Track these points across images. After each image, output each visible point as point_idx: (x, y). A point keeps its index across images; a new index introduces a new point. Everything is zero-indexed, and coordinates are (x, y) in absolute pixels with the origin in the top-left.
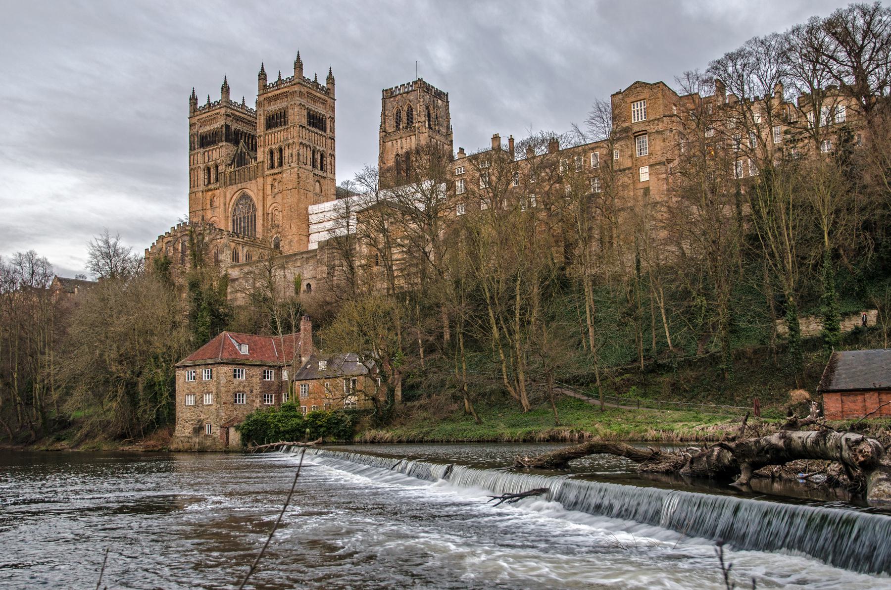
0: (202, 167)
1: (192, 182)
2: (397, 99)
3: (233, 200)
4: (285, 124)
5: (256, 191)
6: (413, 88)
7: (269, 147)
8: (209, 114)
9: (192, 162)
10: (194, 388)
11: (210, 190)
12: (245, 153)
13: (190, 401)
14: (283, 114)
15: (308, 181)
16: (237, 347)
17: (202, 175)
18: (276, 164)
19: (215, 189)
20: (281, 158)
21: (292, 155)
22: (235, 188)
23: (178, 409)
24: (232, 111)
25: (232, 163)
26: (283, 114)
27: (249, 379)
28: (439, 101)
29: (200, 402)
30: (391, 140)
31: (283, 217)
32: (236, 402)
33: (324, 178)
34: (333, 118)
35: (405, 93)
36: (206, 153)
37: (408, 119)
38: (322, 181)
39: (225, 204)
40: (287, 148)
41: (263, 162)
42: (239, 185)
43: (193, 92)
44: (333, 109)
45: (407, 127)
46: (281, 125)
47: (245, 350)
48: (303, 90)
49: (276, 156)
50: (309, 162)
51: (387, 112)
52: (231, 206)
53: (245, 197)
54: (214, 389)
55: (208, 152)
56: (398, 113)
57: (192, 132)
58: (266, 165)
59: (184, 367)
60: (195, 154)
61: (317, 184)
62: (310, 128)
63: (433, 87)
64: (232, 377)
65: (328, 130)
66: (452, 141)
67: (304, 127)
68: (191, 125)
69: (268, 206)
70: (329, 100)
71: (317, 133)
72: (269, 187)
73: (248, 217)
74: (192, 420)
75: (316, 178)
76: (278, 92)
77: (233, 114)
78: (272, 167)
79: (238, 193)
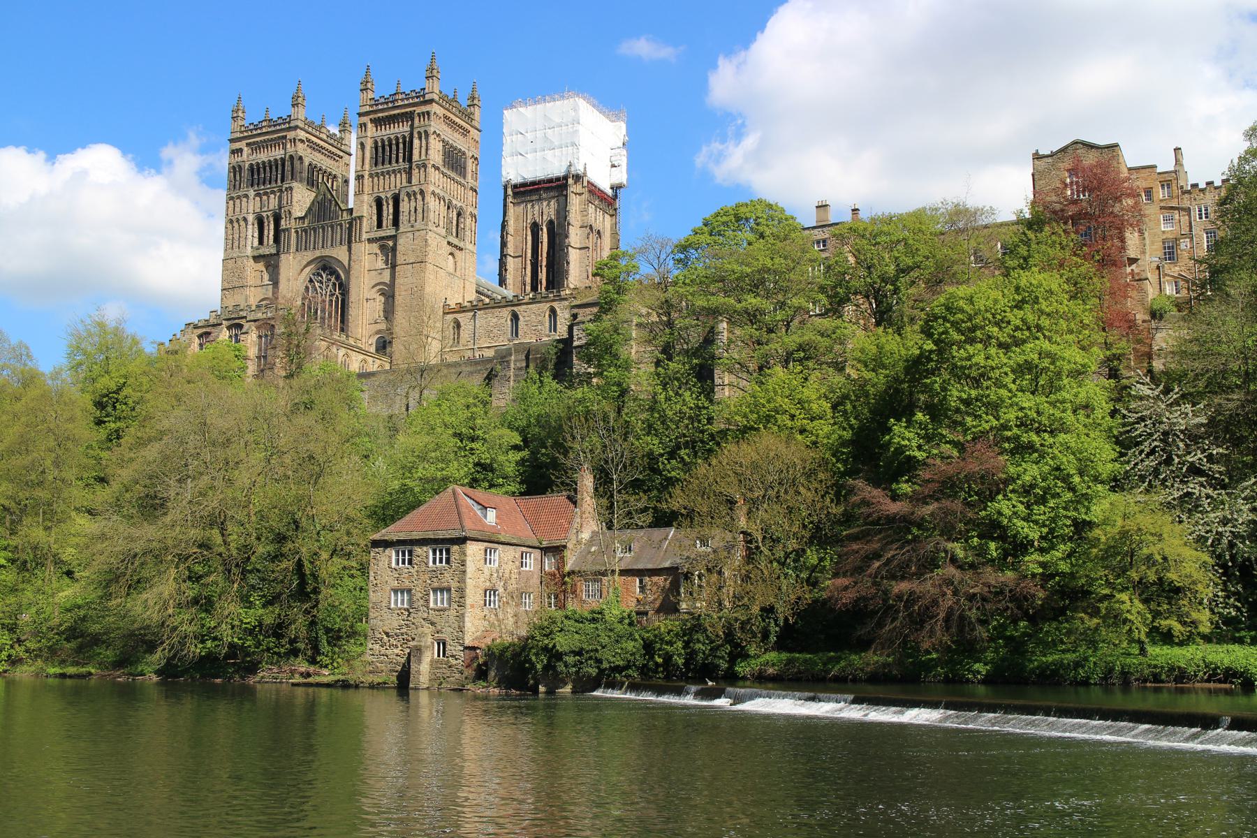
7: (375, 195)
9: (231, 209)
15: (440, 252)
22: (309, 255)
24: (308, 135)
33: (461, 249)
38: (457, 253)
39: (289, 280)
40: (406, 199)
41: (360, 218)
47: (491, 516)
48: (438, 112)
49: (388, 211)
50: (441, 223)
60: (239, 197)
61: (450, 257)
64: (483, 561)
65: (469, 176)
67: (438, 169)
75: (450, 249)
77: (309, 141)
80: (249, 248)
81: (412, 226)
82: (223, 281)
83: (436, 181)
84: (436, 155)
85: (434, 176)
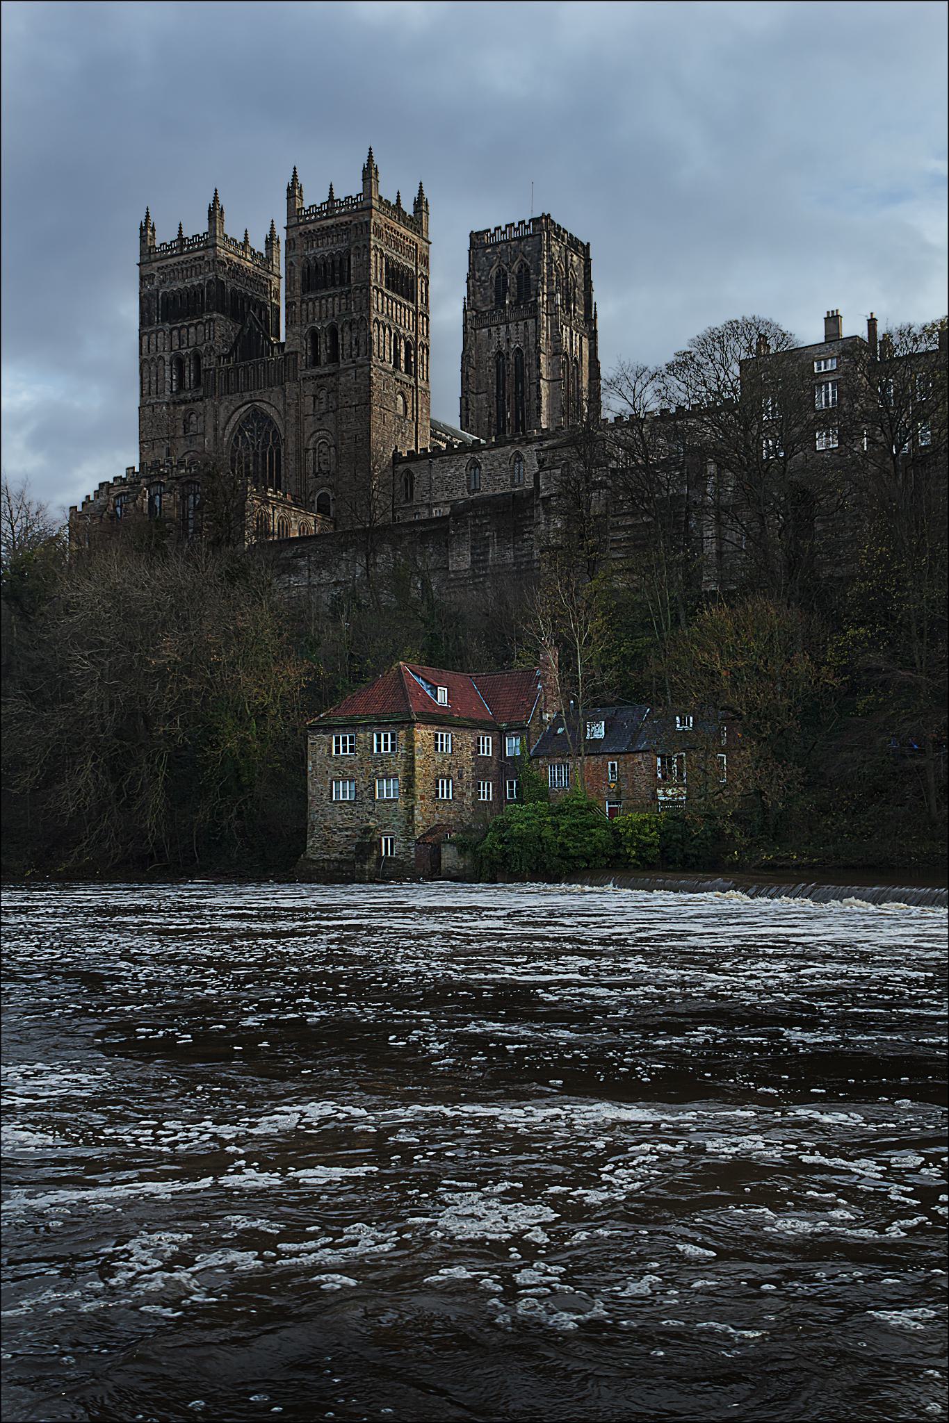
0: (167, 358)
1: (146, 386)
2: (498, 250)
3: (232, 422)
4: (342, 284)
5: (281, 407)
6: (530, 231)
7: (309, 326)
8: (182, 258)
10: (351, 768)
11: (184, 402)
12: (258, 334)
13: (343, 792)
14: (337, 264)
16: (428, 692)
17: (168, 375)
18: (323, 358)
19: (194, 400)
20: (334, 346)
21: (357, 343)
22: (236, 399)
23: (313, 808)
25: (230, 354)
26: (337, 264)
27: (457, 753)
28: (575, 258)
29: (366, 794)
30: (487, 326)
31: (337, 456)
32: (437, 796)
34: (427, 278)
35: (514, 239)
36: (175, 333)
37: (519, 289)
39: (216, 430)
40: (346, 329)
42: (247, 394)
43: (147, 216)
44: (426, 261)
45: (517, 304)
46: (334, 285)
47: (442, 696)
50: (387, 357)
51: (478, 274)
52: (227, 432)
53: (257, 415)
54: (400, 770)
55: (179, 329)
56: (502, 275)
57: (145, 290)
58: (301, 360)
59: (329, 729)
62: (390, 294)
63: (565, 231)
66: (596, 331)
68: (142, 278)
69: (307, 434)
70: (419, 241)
71: (400, 304)
72: (309, 400)
73: (264, 454)
74: (347, 829)
76: (330, 222)
78: (315, 362)
79: (242, 410)
80: (168, 393)
81: (354, 362)
82: (141, 433)
83: (382, 304)
84: (377, 275)
85: (377, 301)
